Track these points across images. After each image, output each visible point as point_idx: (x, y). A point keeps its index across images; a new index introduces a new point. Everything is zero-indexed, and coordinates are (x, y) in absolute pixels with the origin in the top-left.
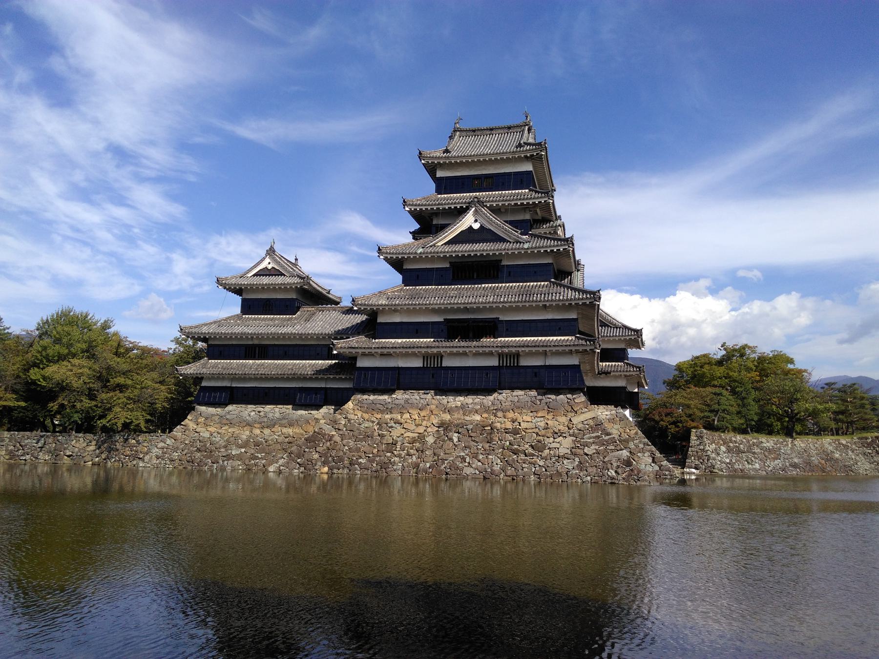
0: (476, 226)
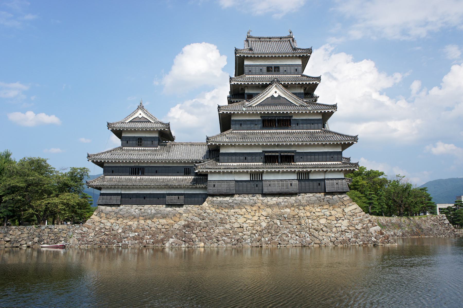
0: (276, 95)
